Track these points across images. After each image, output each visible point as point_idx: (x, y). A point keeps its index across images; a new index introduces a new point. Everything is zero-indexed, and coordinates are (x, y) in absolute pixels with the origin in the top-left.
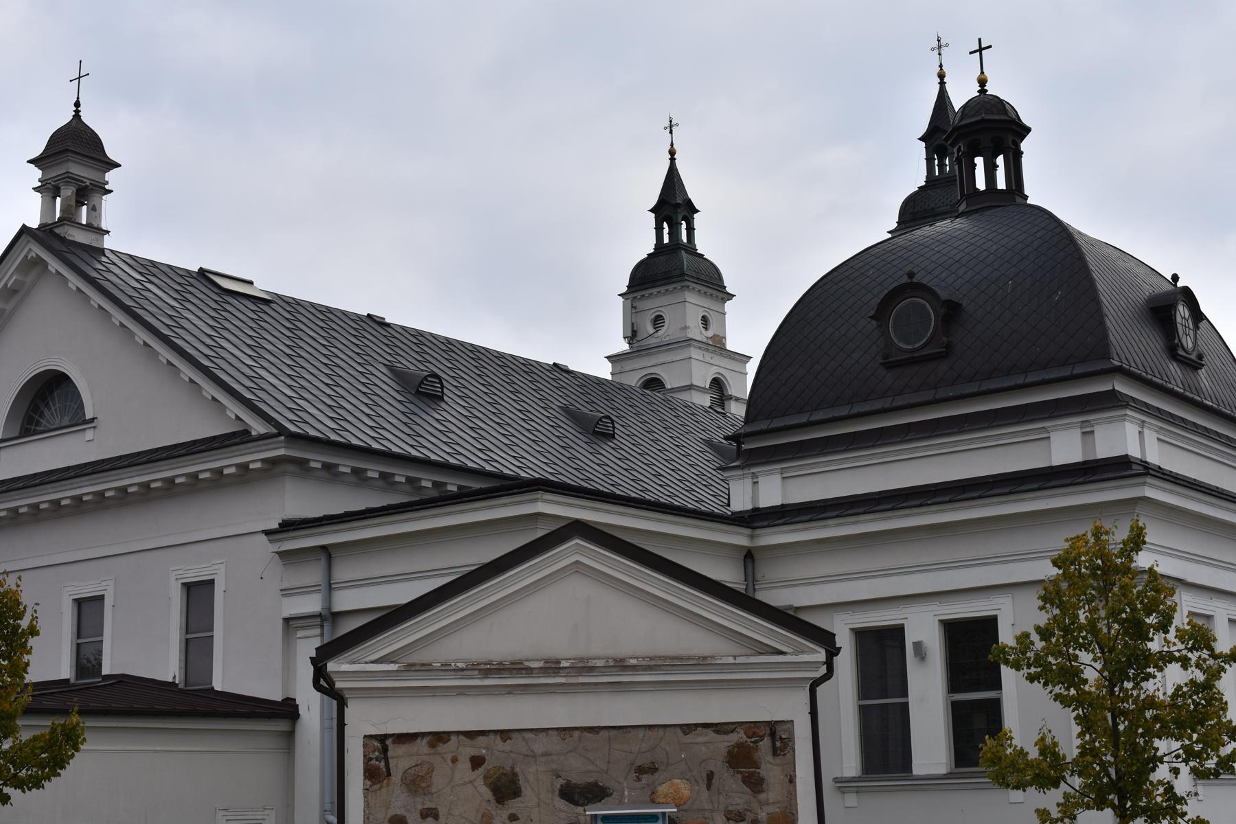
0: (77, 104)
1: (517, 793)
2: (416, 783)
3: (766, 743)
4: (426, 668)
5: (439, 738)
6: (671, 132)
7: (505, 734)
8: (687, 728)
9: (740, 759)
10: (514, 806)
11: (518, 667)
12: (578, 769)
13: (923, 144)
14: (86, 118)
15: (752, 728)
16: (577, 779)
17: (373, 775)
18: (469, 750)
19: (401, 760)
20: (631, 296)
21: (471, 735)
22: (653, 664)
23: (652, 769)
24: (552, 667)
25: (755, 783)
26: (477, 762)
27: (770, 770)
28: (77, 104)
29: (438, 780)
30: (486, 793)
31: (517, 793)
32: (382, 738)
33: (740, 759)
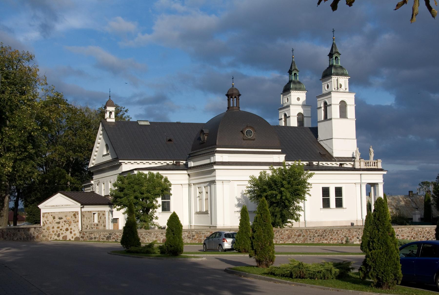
0: (110, 97)
1: (55, 218)
2: (47, 217)
3: (76, 214)
4: (48, 206)
5: (49, 213)
6: (293, 52)
7: (54, 213)
8: (70, 212)
9: (74, 215)
10: (55, 220)
11: (53, 206)
12: (60, 216)
13: (329, 57)
14: (111, 99)
15: (75, 212)
16: (60, 217)
17: (43, 216)
18: (51, 214)
19: (45, 215)
20: (284, 94)
21: (51, 213)
22: (65, 205)
23: (66, 216)
24: (57, 206)
25: (76, 217)
26: (52, 215)
27: (77, 216)
28: (110, 97)
29: (48, 217)
30: (53, 219)
31: (55, 218)
32: (44, 213)
33: (74, 215)
